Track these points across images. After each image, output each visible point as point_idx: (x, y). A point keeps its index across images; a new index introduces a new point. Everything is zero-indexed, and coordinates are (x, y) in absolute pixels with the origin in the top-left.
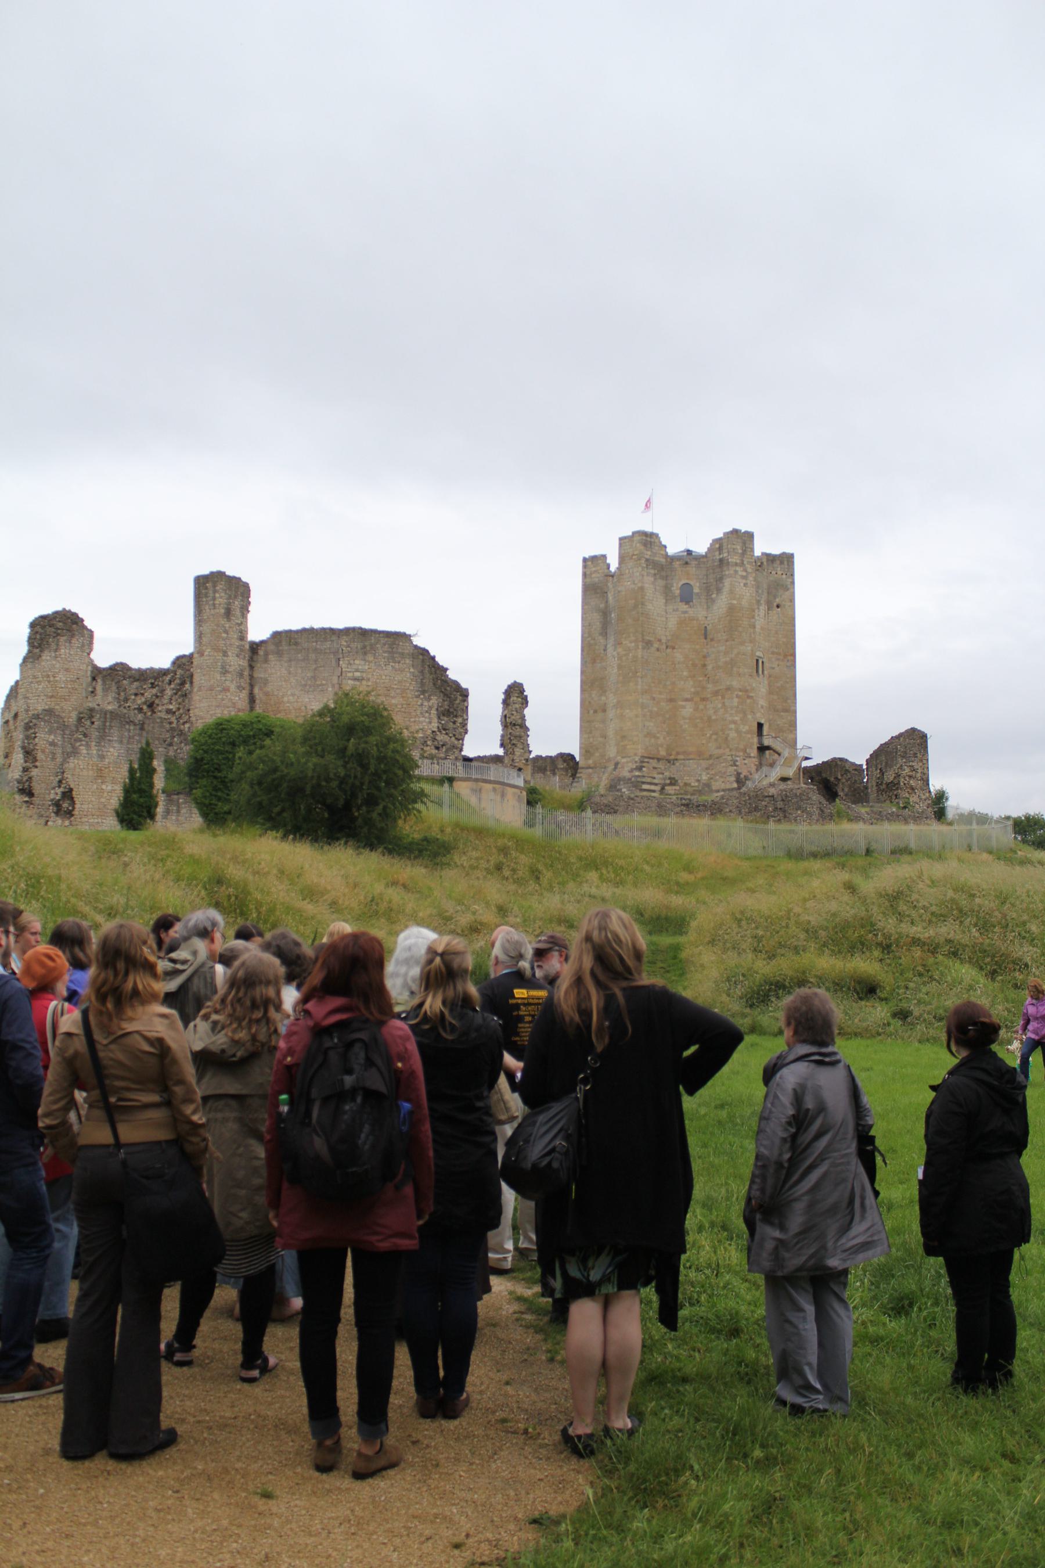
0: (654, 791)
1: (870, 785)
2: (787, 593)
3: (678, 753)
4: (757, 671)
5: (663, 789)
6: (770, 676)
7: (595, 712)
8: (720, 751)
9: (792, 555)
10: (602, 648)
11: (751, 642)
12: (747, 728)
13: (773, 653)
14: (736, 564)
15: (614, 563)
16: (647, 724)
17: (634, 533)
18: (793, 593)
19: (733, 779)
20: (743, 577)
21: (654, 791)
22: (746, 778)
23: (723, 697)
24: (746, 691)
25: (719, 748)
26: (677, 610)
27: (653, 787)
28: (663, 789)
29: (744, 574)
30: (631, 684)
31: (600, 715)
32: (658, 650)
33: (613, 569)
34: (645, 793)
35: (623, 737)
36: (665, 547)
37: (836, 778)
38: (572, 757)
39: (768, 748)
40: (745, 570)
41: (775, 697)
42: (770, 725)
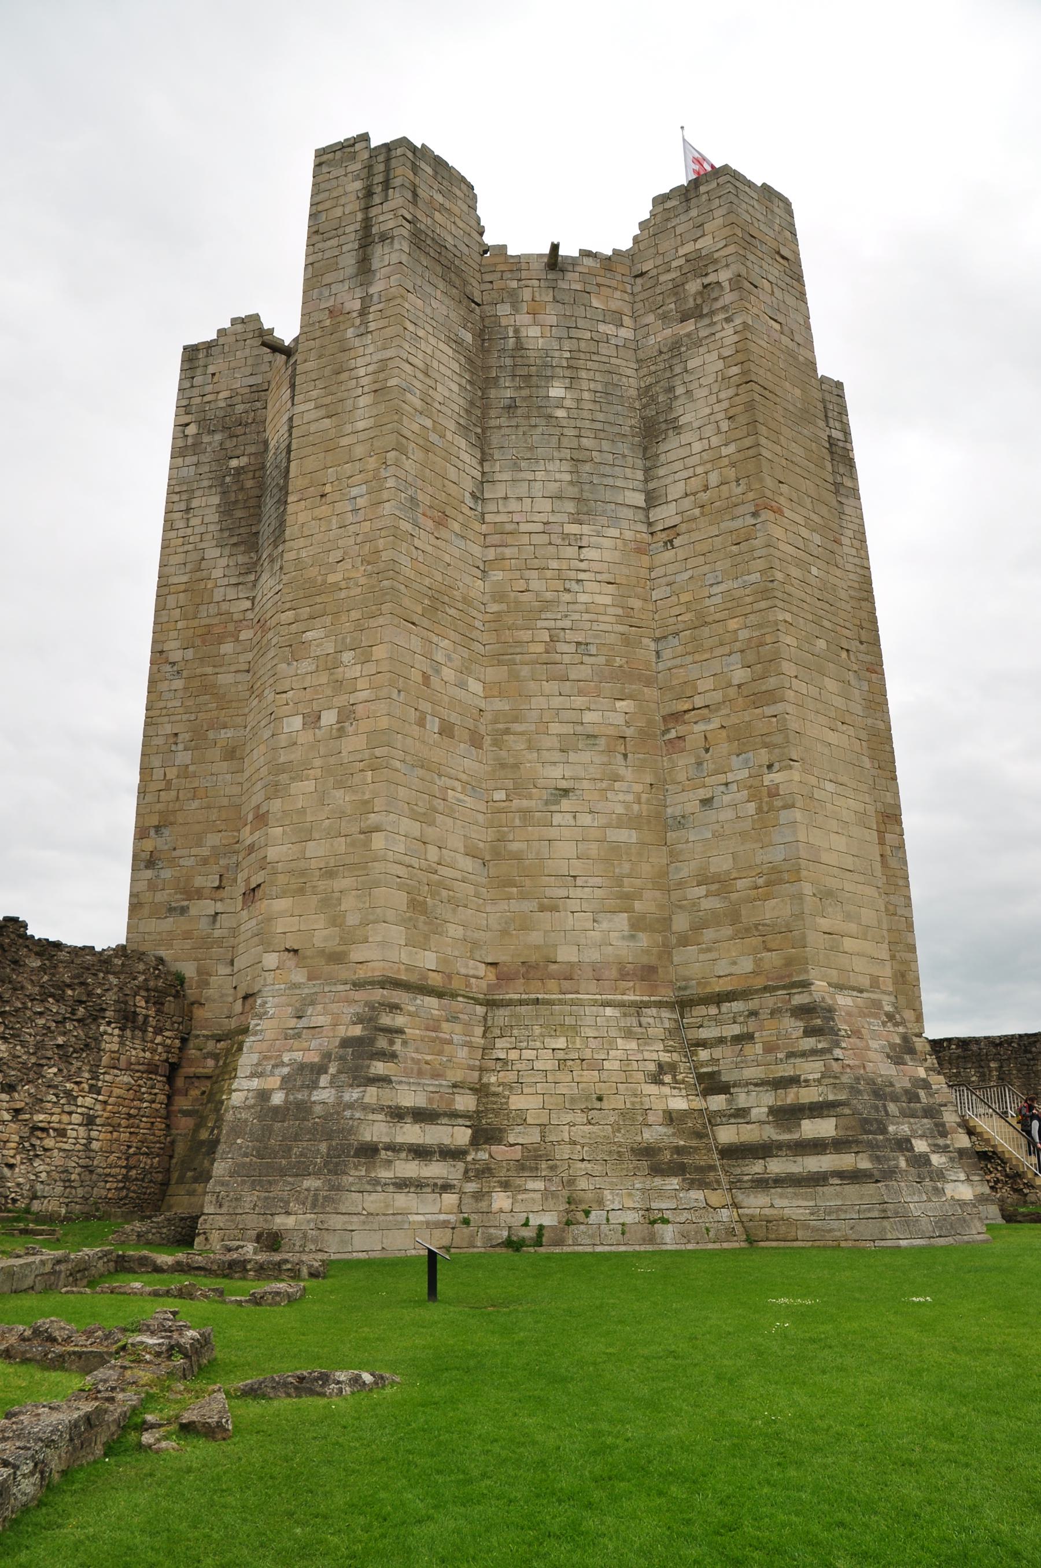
7: (446, 730)
10: (469, 485)
35: (826, 895)
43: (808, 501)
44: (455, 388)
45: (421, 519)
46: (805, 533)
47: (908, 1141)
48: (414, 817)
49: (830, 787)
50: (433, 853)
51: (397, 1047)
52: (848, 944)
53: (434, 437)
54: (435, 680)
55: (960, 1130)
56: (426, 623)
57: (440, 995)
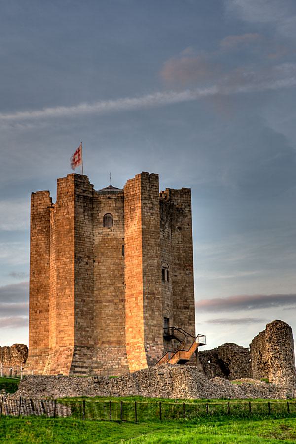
0: (85, 373)
1: (253, 364)
2: (186, 219)
3: (103, 343)
4: (164, 279)
5: (91, 371)
6: (174, 282)
9: (190, 189)
11: (157, 257)
12: (155, 322)
13: (175, 264)
15: (54, 195)
16: (79, 320)
17: (68, 175)
18: (191, 218)
19: (145, 361)
20: (151, 208)
21: (85, 373)
23: (136, 299)
24: (154, 294)
25: (134, 338)
27: (83, 370)
28: (91, 371)
29: (151, 205)
31: (45, 314)
32: (87, 264)
33: (54, 201)
34: (77, 374)
36: (92, 186)
37: (228, 359)
38: (26, 346)
39: (173, 337)
40: (152, 203)
41: (178, 298)
42: (174, 320)
43: (67, 252)
44: (43, 244)
45: (35, 276)
46: (65, 260)
47: (59, 372)
48: (34, 328)
49: (64, 311)
50: (38, 333)
51: (29, 365)
52: (65, 339)
53: (38, 258)
54: (39, 304)
56: (37, 294)
57: (38, 356)
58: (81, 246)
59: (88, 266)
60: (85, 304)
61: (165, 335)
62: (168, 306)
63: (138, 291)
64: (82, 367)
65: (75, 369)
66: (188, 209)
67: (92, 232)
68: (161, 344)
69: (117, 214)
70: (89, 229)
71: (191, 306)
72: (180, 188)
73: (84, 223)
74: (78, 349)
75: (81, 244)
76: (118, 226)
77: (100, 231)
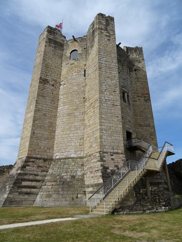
6: (134, 105)
8: (92, 149)
14: (102, 29)
20: (106, 36)
22: (113, 173)
26: (68, 64)
29: (108, 34)
30: (31, 106)
41: (139, 118)
55: (100, 178)
58: (48, 72)
59: (53, 87)
60: (46, 117)
61: (128, 147)
62: (130, 122)
63: (95, 100)
64: (32, 181)
65: (21, 183)
66: (142, 58)
67: (61, 64)
68: (122, 154)
69: (81, 49)
70: (58, 62)
71: (151, 124)
72: (134, 46)
73: (54, 57)
74: (32, 160)
75: (48, 70)
76: (81, 57)
77: (67, 63)
